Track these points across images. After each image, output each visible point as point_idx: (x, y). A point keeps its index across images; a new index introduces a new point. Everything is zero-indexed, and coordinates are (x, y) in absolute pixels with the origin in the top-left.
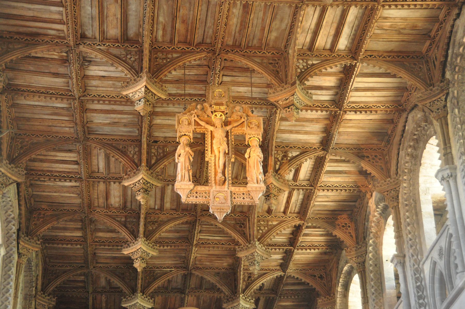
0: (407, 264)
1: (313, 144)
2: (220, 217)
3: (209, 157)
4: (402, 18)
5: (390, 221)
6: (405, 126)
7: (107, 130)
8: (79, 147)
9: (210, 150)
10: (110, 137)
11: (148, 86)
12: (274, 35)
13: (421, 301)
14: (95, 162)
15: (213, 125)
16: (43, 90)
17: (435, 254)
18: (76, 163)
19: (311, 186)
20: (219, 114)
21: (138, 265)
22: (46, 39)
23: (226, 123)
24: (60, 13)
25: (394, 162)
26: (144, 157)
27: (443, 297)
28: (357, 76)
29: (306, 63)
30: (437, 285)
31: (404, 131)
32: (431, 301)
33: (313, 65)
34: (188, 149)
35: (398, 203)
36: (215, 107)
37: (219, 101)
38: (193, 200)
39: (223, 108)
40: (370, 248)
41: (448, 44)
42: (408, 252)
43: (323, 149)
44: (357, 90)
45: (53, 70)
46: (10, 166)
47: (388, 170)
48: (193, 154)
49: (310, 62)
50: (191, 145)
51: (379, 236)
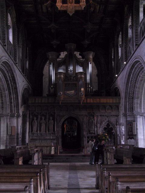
0: (134, 28)
2: (71, 14)
17: (142, 25)
21: (53, 31)
38: (62, 9)
42: (134, 25)
51: (128, 19)
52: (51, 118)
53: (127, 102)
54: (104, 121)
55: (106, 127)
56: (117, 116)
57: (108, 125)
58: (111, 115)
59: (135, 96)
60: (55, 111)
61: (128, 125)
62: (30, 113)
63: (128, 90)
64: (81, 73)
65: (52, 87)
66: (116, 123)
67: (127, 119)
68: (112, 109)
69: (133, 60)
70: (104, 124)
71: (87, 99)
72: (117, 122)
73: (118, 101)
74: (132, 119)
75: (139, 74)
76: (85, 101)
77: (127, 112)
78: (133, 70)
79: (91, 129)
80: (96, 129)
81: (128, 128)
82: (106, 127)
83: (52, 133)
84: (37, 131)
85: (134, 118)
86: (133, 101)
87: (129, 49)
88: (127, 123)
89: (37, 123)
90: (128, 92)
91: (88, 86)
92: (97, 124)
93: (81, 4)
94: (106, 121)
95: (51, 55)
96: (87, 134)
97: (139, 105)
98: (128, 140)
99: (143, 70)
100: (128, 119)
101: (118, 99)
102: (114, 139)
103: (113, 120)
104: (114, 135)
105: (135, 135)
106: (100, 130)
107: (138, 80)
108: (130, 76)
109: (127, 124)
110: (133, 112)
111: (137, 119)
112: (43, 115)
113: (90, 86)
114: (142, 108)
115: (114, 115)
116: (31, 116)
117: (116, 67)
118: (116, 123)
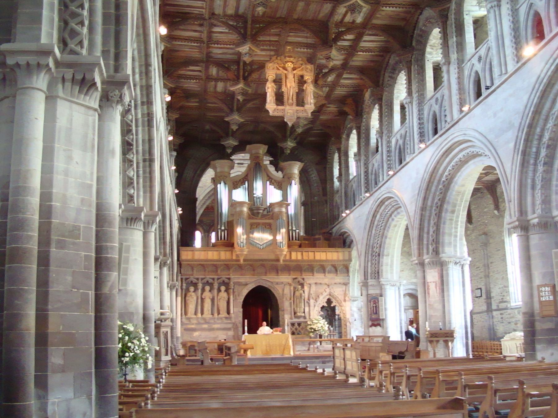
1: (337, 65)
3: (284, 89)
4: (392, 11)
5: (377, 106)
6: (389, 60)
7: (219, 56)
8: (204, 65)
9: (284, 85)
10: (221, 60)
11: (251, 47)
12: (321, 15)
13: (389, 158)
14: (210, 70)
15: (286, 70)
16: (187, 38)
17: (398, 136)
18: (200, 71)
19: (334, 85)
20: (290, 64)
22: (192, 15)
23: (294, 69)
24: (203, 4)
25: (382, 78)
26: (241, 74)
27: (401, 162)
28: (366, 35)
29: (338, 30)
30: (397, 151)
31: (388, 62)
32: (394, 159)
33: (342, 31)
34: (273, 84)
35: (382, 102)
36: (288, 59)
37: (289, 55)
38: (276, 114)
39: (292, 59)
40: (364, 120)
41: (415, 27)
43: (343, 68)
44: (365, 41)
45: (193, 29)
46: (168, 78)
47: (378, 82)
48: (275, 87)
49: (340, 30)
50: (275, 81)
52: (223, 288)
53: (368, 261)
54: (322, 294)
55: (326, 305)
56: (346, 284)
57: (329, 301)
58: (335, 284)
59: (383, 251)
60: (231, 275)
61: (370, 302)
62: (182, 279)
63: (370, 241)
64: (280, 204)
65: (223, 228)
66: (345, 297)
67: (367, 291)
68: (336, 271)
69: (383, 193)
70: (322, 302)
71: (291, 254)
72: (345, 295)
73: (347, 258)
74: (378, 292)
75: (391, 215)
76: (288, 258)
77: (368, 279)
78: (383, 208)
79: (298, 309)
80: (307, 309)
81: (371, 308)
82: (326, 305)
83: (226, 318)
84: (196, 313)
85: (381, 289)
86: (379, 259)
87: (373, 168)
88: (369, 299)
89: (195, 298)
90: (371, 244)
91: (290, 228)
92: (309, 299)
93: (307, 107)
94: (325, 294)
95: (221, 164)
96: (291, 318)
97: (389, 266)
98: (370, 329)
99: (399, 210)
100: (371, 292)
101: (347, 253)
102: (340, 326)
103: (338, 292)
104: (340, 319)
105: (383, 320)
106: (315, 311)
107: (390, 225)
108: (376, 216)
109: (368, 300)
110: (380, 280)
111: (385, 292)
112: (208, 283)
113: (294, 229)
114: (395, 271)
115: (340, 283)
116: (184, 285)
117: (345, 193)
118: (345, 297)
